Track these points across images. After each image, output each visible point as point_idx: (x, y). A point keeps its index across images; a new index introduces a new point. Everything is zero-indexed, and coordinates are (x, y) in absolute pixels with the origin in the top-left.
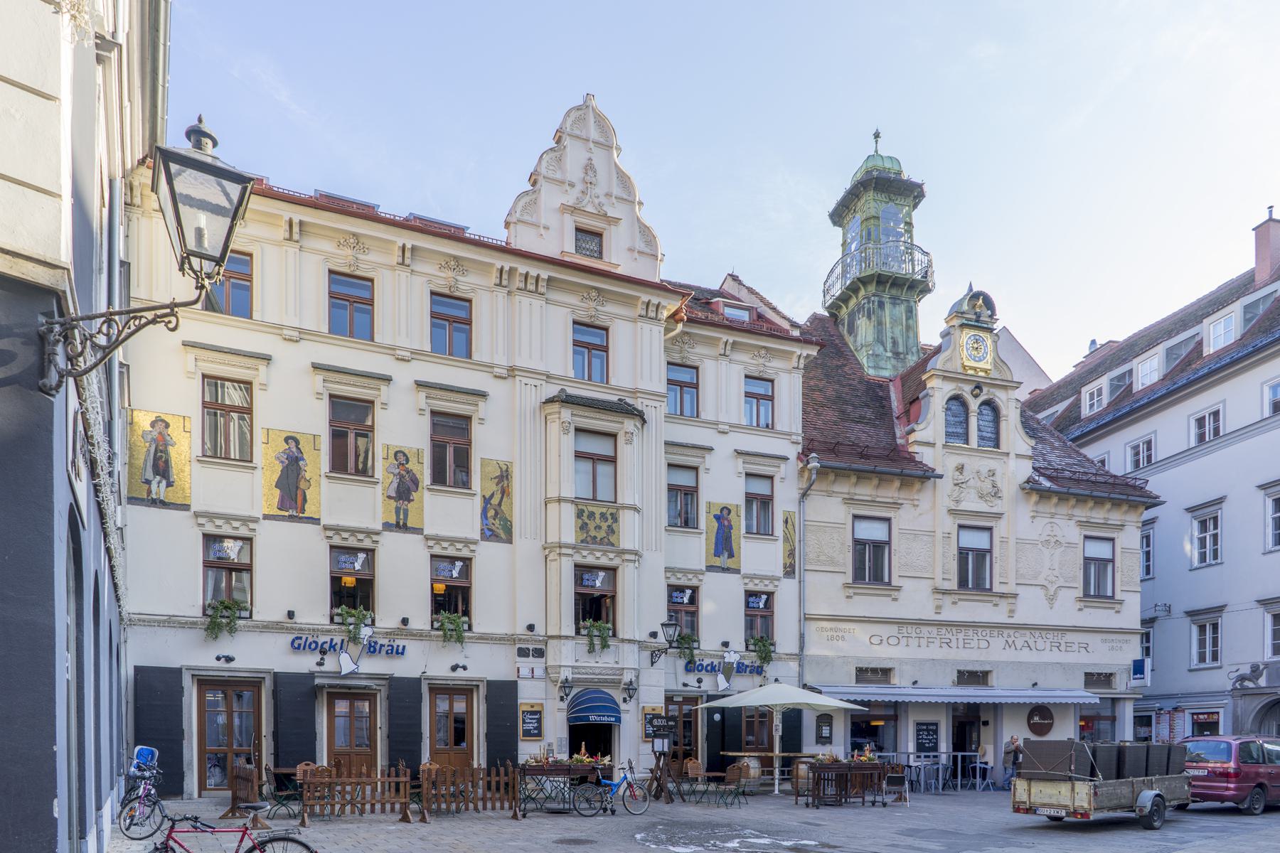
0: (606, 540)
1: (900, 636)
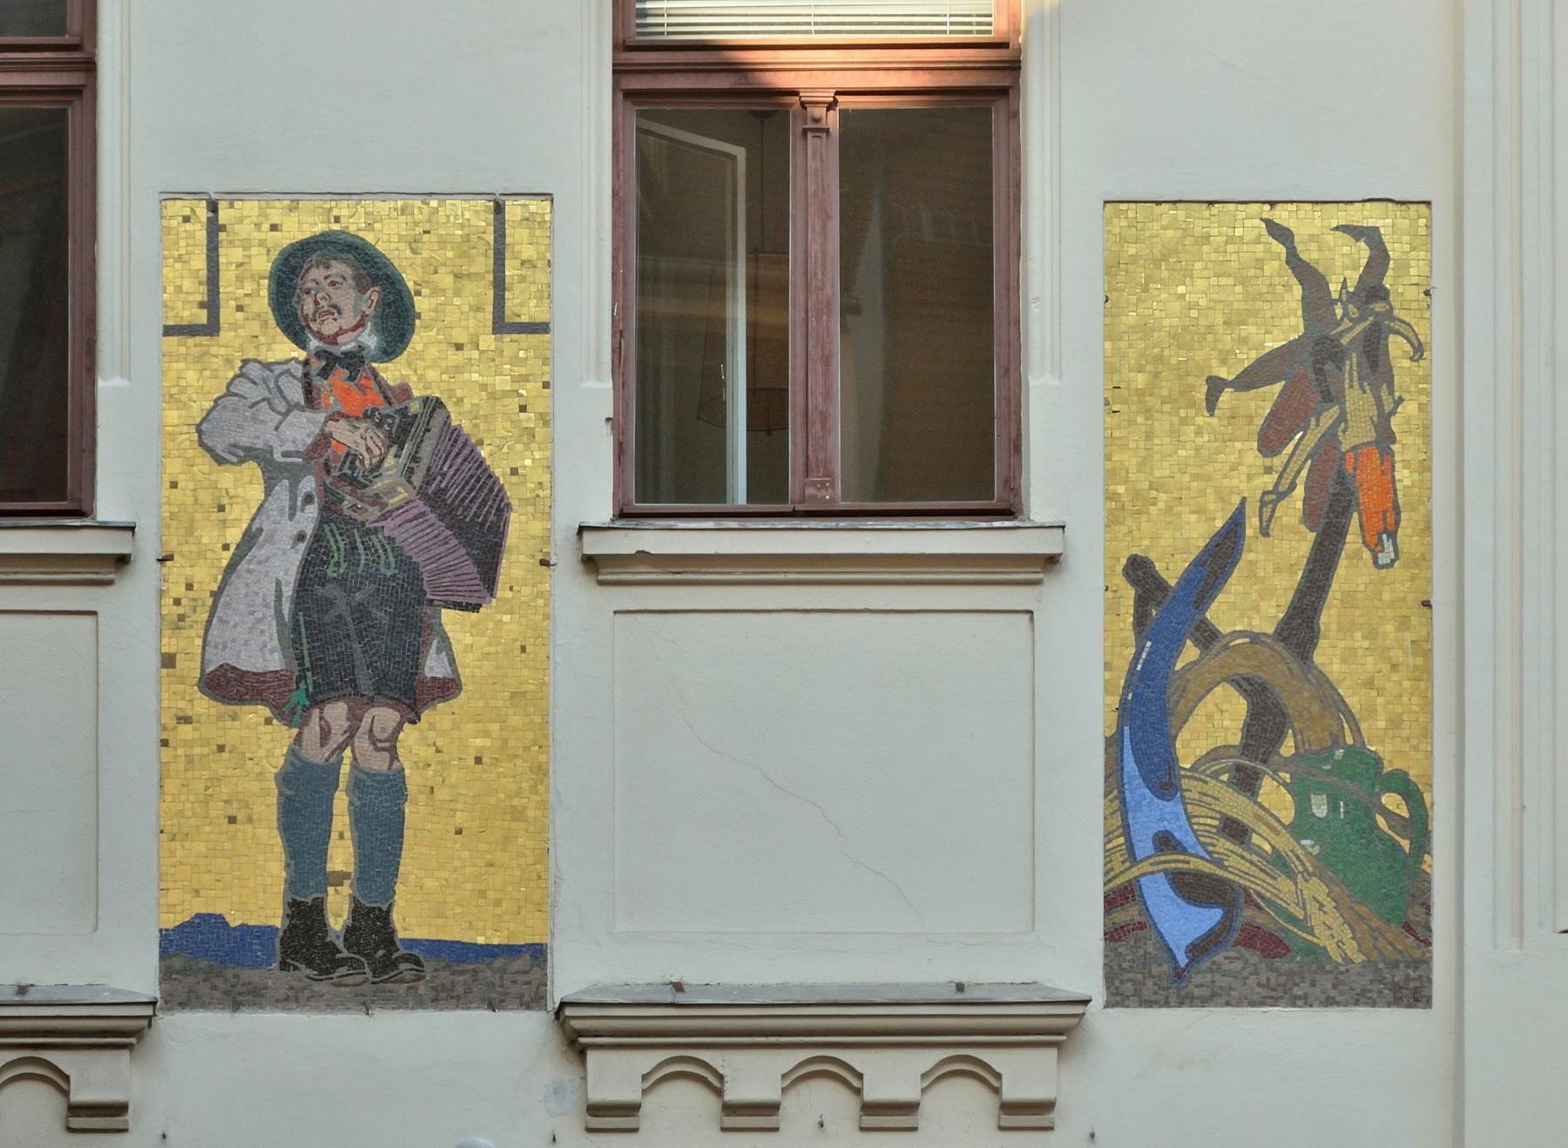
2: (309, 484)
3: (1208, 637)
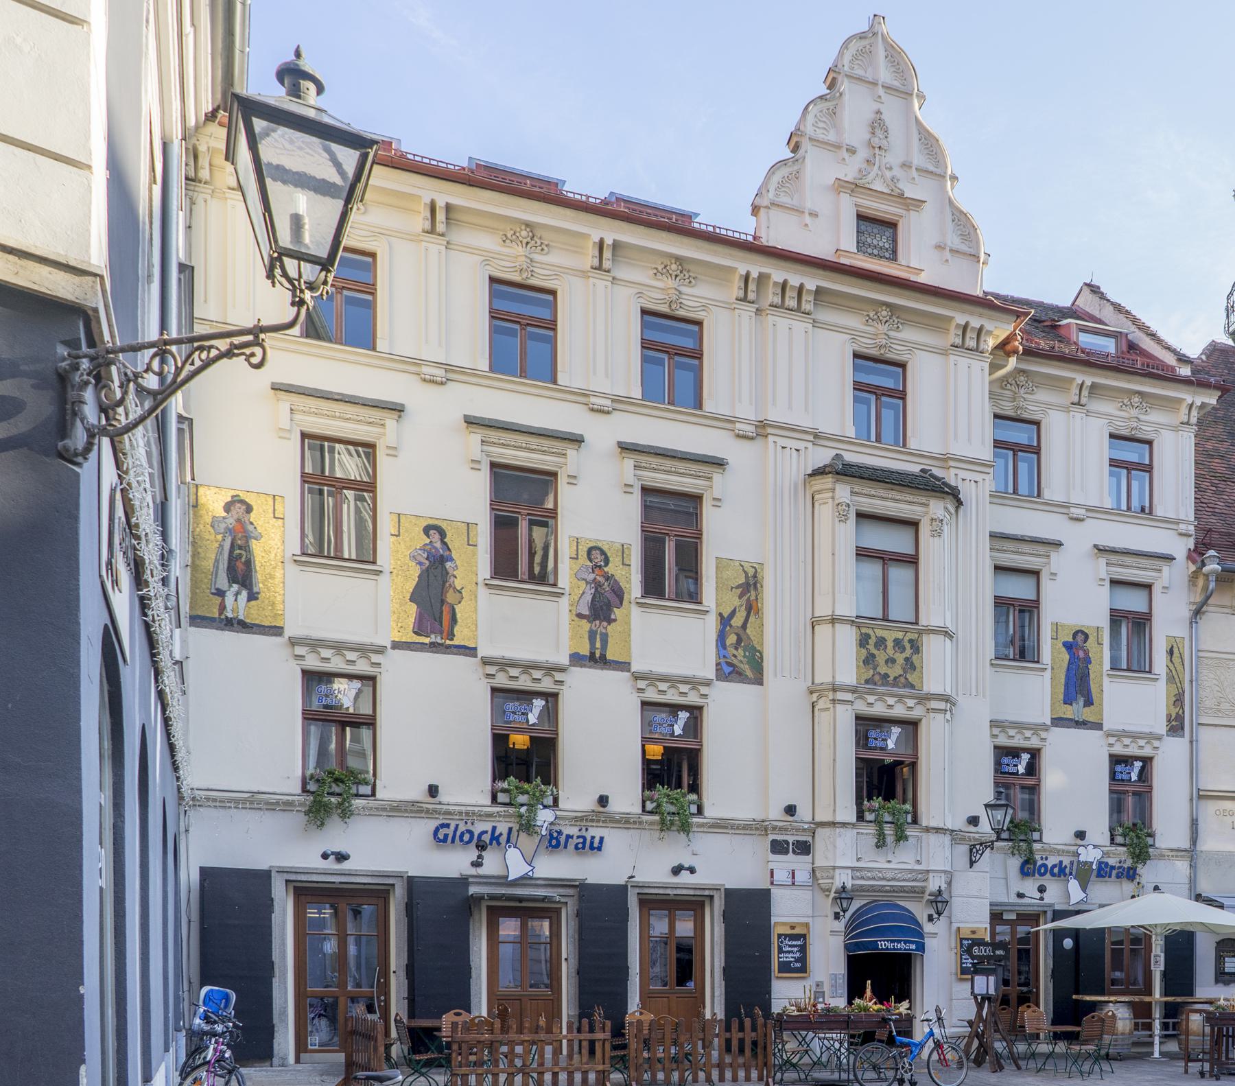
0: (902, 679)
2: (593, 585)
3: (731, 626)
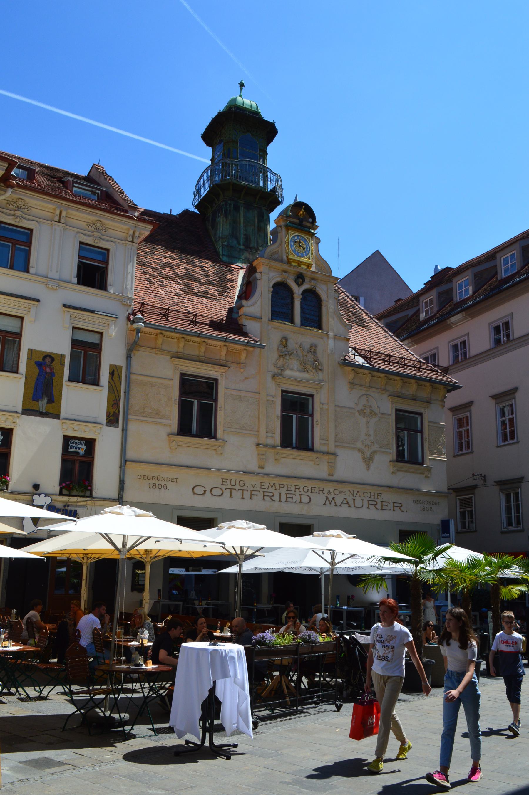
1: (224, 488)
